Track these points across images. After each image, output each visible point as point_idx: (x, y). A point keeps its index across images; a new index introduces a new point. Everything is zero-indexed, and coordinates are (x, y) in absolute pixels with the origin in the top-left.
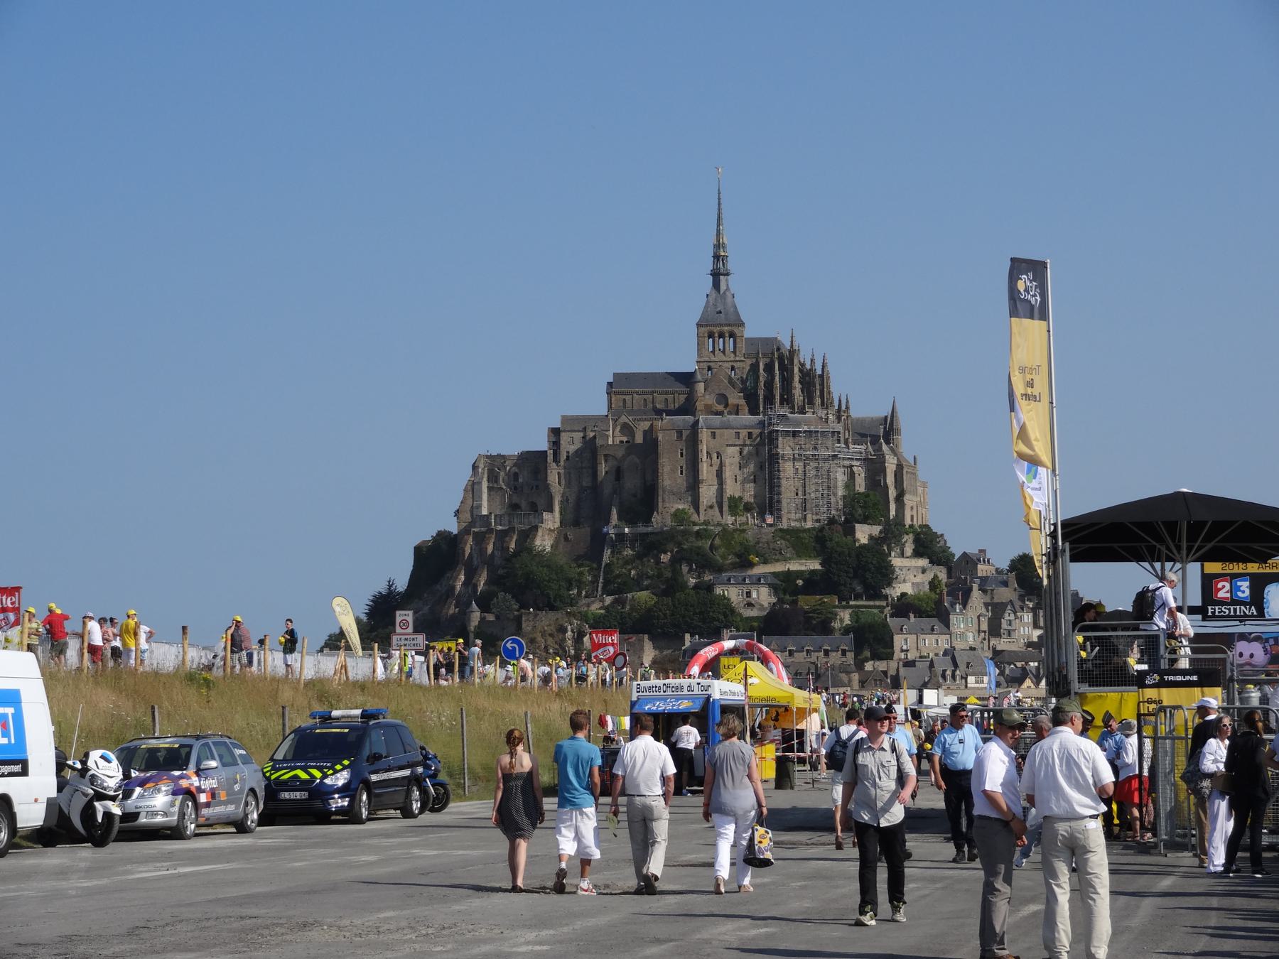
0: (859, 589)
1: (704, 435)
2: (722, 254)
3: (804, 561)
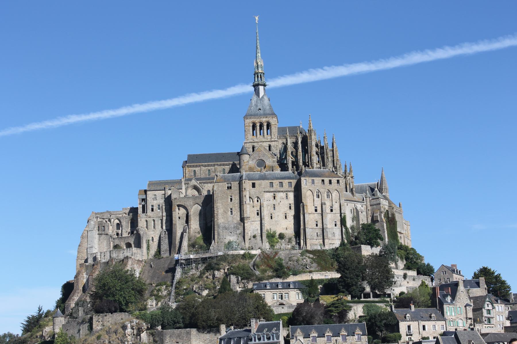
0: (368, 289)
1: (247, 185)
2: (261, 72)
3: (324, 272)
